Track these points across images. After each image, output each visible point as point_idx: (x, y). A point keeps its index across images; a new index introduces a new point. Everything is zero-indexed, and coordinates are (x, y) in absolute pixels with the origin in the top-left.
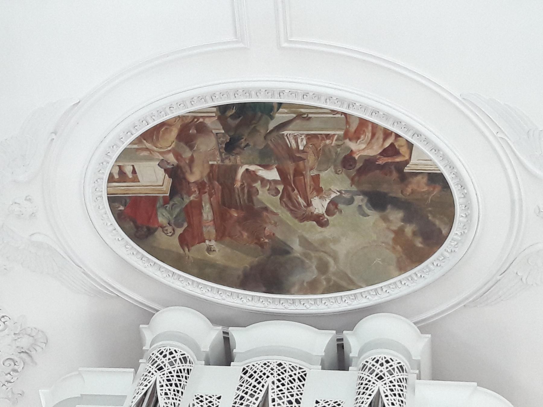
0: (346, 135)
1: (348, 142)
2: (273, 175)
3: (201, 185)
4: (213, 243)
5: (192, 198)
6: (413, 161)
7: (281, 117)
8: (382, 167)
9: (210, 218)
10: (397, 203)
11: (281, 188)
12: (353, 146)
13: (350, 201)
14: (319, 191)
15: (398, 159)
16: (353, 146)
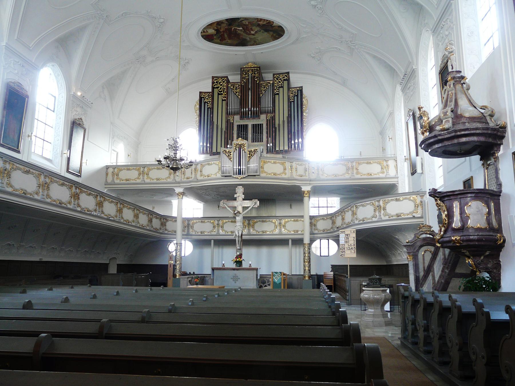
0: (258, 21)
1: (258, 22)
2: (241, 28)
3: (223, 32)
4: (228, 40)
5: (222, 34)
6: (274, 24)
7: (241, 19)
8: (266, 25)
9: (227, 36)
10: (271, 31)
11: (243, 30)
12: (260, 23)
13: (260, 31)
14: (252, 30)
15: (271, 24)
16: (260, 23)
